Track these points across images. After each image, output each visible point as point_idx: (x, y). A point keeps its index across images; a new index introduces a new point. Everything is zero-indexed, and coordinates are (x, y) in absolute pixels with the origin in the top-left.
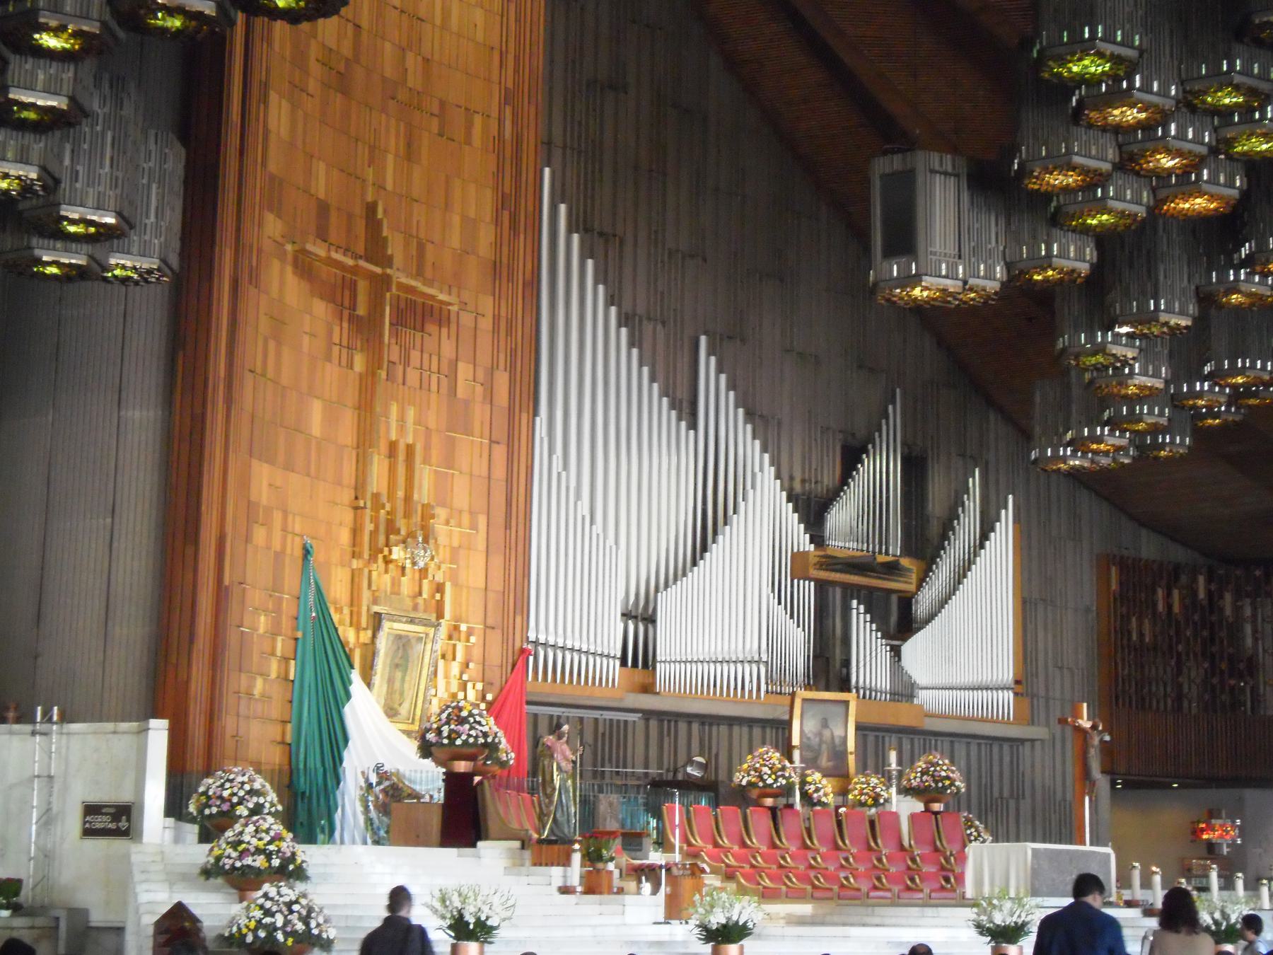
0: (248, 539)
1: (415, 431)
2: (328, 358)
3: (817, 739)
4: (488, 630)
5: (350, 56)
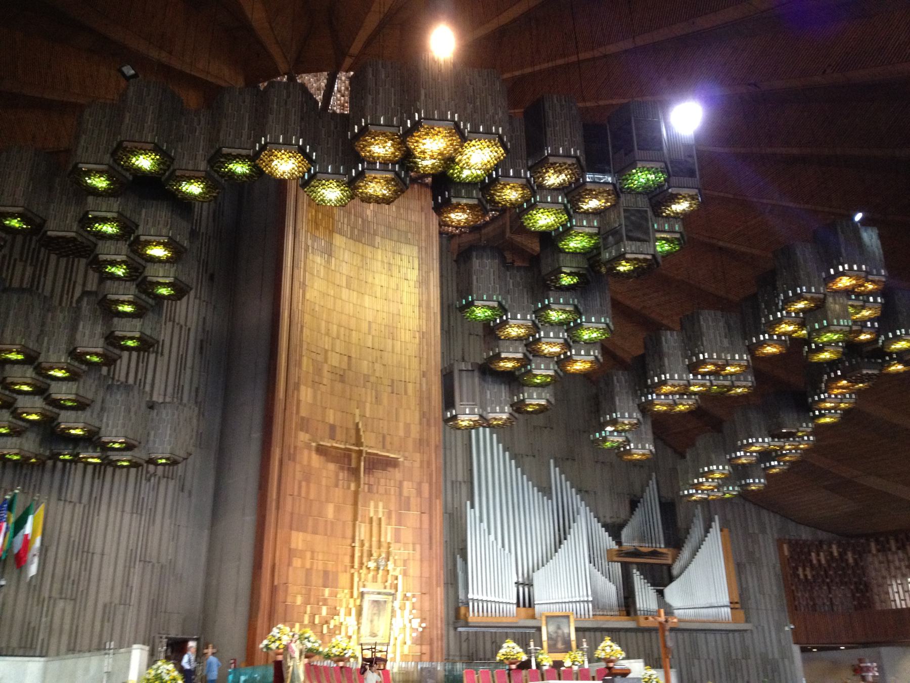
0: (289, 564)
1: (383, 512)
2: (337, 486)
4: (423, 595)
5: (346, 367)
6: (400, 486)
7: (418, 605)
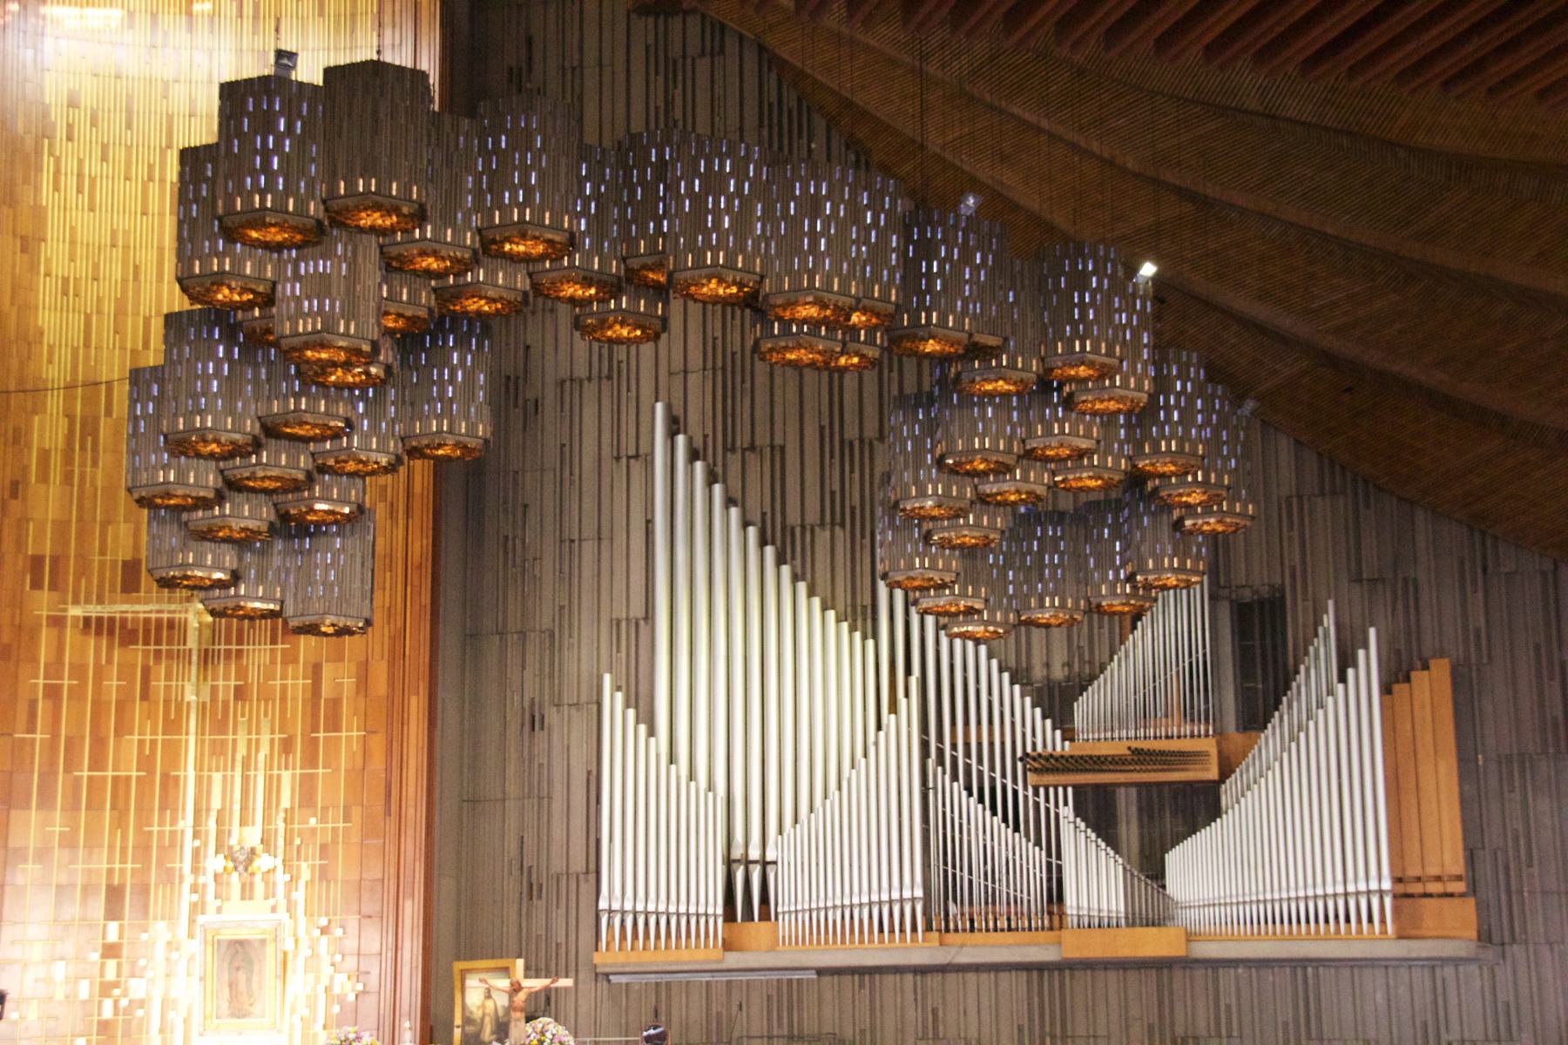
3: (480, 1012)
6: (316, 671)
7: (351, 944)
